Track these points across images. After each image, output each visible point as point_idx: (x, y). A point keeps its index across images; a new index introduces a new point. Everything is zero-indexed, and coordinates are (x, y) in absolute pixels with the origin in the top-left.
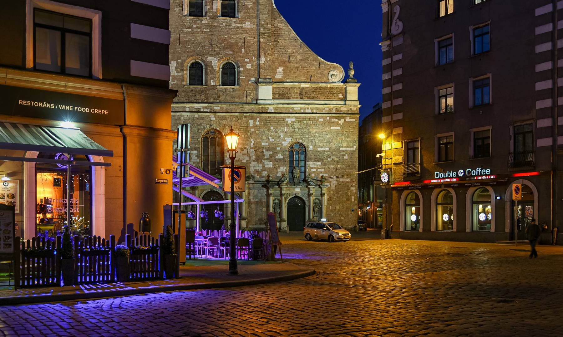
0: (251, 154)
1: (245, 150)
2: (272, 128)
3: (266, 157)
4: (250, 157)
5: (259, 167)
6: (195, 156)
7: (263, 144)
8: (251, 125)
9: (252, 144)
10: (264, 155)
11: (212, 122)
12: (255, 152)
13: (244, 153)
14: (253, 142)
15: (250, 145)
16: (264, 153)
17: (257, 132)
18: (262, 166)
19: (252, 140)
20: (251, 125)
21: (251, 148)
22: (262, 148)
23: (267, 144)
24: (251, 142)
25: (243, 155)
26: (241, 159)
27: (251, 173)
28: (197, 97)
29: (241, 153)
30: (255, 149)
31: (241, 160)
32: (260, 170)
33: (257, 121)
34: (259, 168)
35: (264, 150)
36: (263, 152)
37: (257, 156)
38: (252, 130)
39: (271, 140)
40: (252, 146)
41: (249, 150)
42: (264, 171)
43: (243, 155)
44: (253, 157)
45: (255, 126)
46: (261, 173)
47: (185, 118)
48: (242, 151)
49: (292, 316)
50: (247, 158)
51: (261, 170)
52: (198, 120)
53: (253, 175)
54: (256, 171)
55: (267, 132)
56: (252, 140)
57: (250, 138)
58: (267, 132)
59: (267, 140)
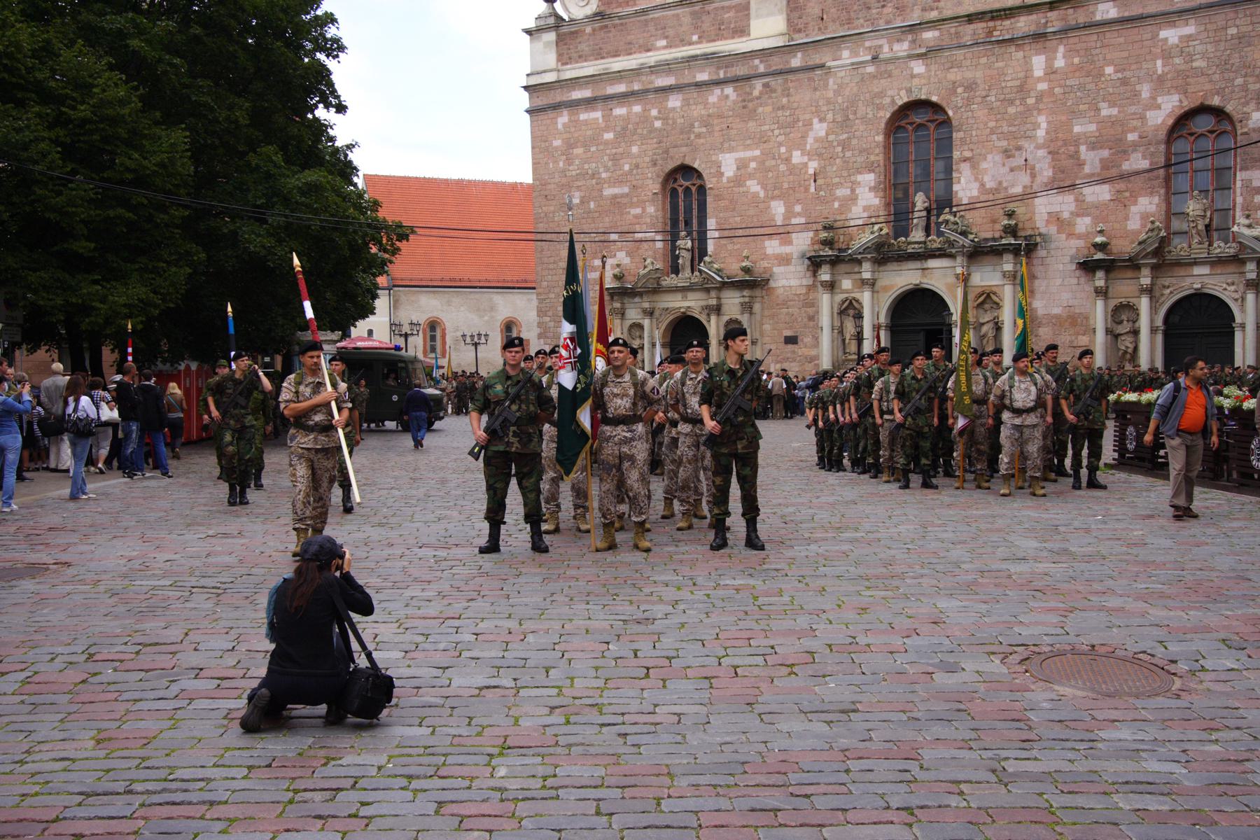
0: (1037, 166)
1: (1017, 153)
2: (1109, 70)
3: (1087, 169)
4: (1033, 176)
5: (1064, 204)
6: (867, 189)
7: (1077, 129)
8: (1038, 73)
9: (1041, 133)
10: (1081, 164)
11: (916, 81)
12: (1050, 156)
13: (1013, 165)
14: (1044, 125)
15: (1035, 136)
16: (1083, 157)
17: (1057, 90)
18: (1077, 200)
19: (1042, 120)
20: (1038, 73)
21: (1038, 147)
22: (1077, 143)
23: (1093, 127)
24: (1036, 126)
25: (1012, 170)
26: (1005, 184)
27: (1037, 217)
28: (874, 11)
29: (1004, 165)
30: (1051, 149)
31: (1006, 188)
32: (1066, 215)
33: (1060, 55)
34: (1064, 207)
35: (1083, 148)
36: (1077, 152)
37: (1059, 170)
38: (1043, 86)
39: (1104, 112)
40: (1041, 141)
41: (1031, 152)
42: (1083, 215)
43: (1012, 170)
44: (1045, 174)
45: (1051, 72)
46: (1071, 224)
47: (839, 81)
48: (1009, 157)
49: (25, 766)
50: (1025, 179)
51: (1072, 213)
52: (876, 82)
53: (1043, 230)
54: (1055, 218)
55: (1092, 86)
56: (1042, 120)
57: (1035, 113)
58: (1092, 86)
59: (1092, 114)
